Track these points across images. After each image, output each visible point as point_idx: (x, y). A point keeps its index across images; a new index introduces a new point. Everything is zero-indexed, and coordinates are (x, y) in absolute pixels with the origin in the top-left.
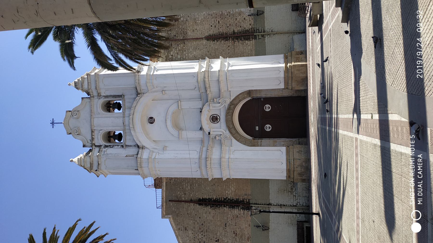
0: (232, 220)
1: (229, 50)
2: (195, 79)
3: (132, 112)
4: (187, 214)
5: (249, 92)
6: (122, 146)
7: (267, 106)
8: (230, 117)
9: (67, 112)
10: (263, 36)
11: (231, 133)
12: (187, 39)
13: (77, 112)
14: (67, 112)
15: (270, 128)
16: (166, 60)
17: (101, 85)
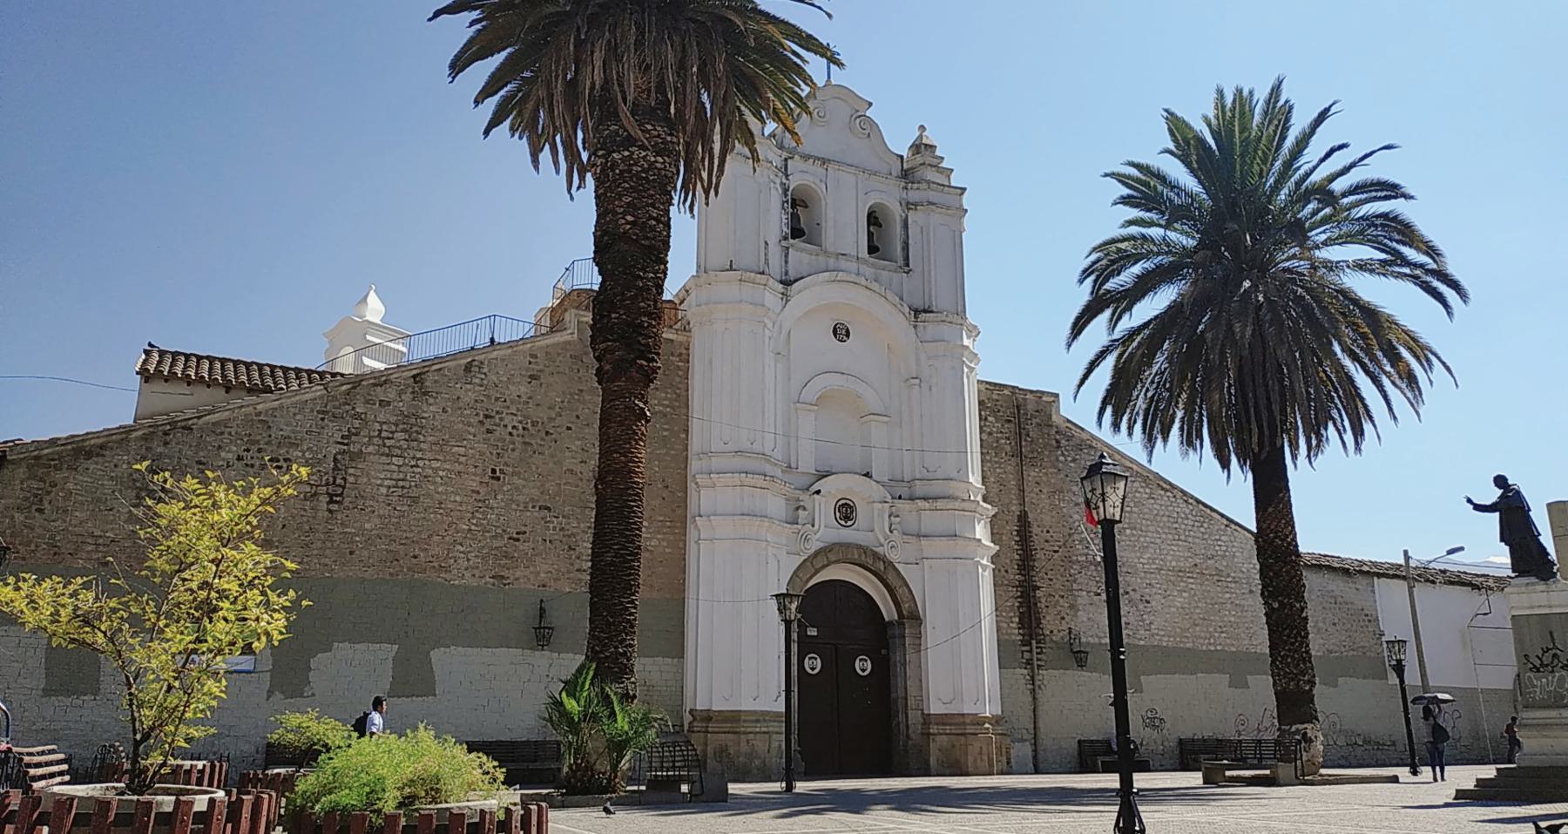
2: (954, 474)
3: (875, 286)
5: (916, 618)
9: (870, 104)
10: (1029, 662)
11: (817, 553)
14: (870, 104)
16: (981, 403)
17: (936, 217)
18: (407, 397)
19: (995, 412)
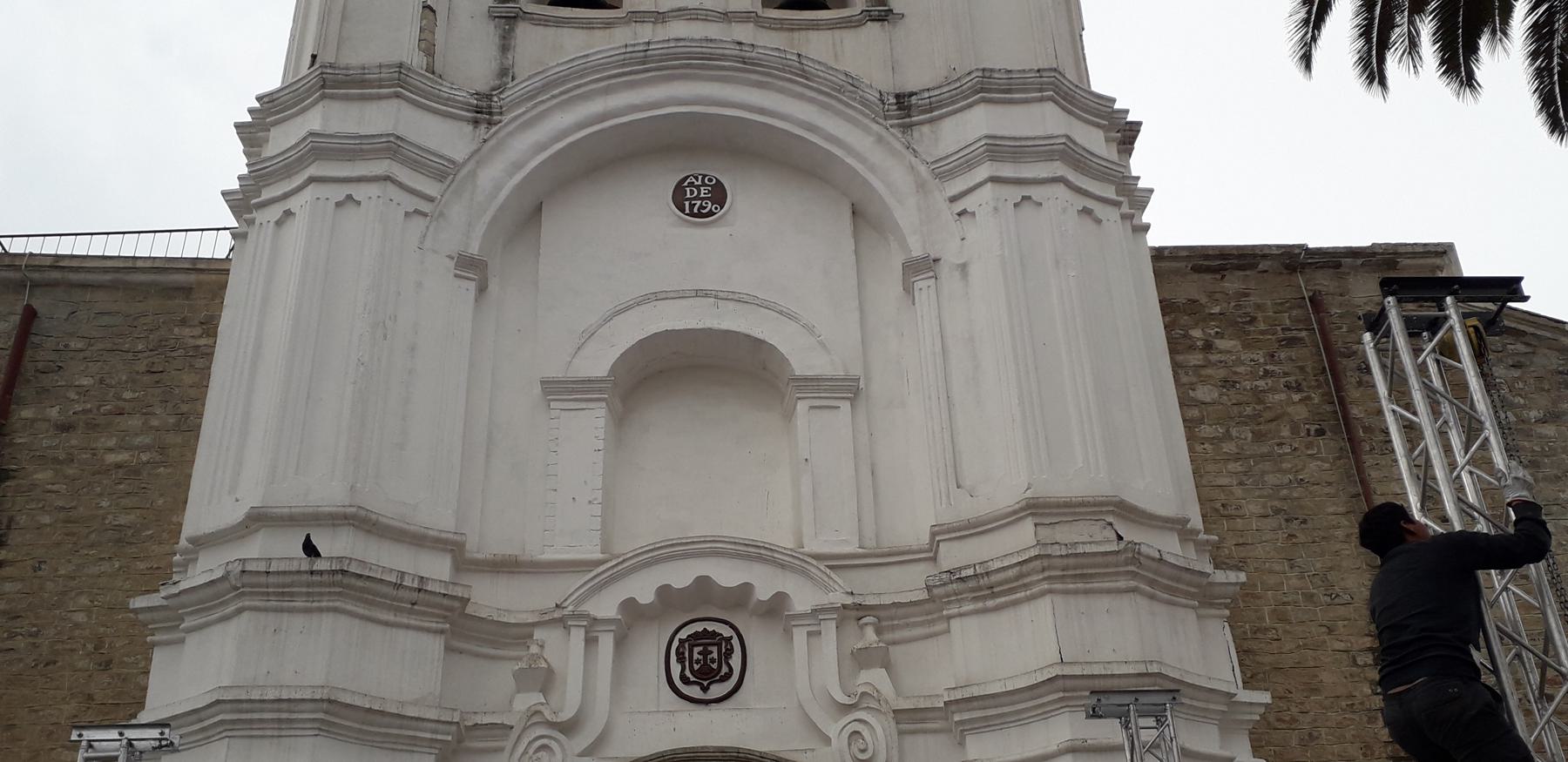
16: (1167, 307)
19: (1240, 325)
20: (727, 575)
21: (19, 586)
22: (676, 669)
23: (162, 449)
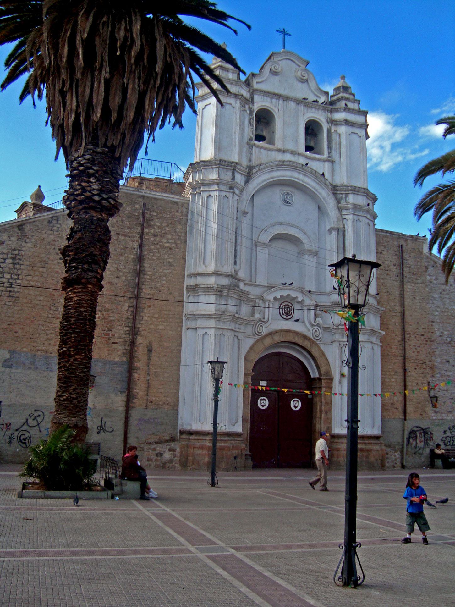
0: (104, 318)
1: (386, 347)
4: (118, 234)
6: (250, 140)
7: (299, 404)
8: (291, 338)
12: (402, 281)
13: (305, 78)
15: (263, 406)
18: (14, 239)
20: (293, 294)
21: (151, 273)
22: (281, 312)
23: (176, 244)
